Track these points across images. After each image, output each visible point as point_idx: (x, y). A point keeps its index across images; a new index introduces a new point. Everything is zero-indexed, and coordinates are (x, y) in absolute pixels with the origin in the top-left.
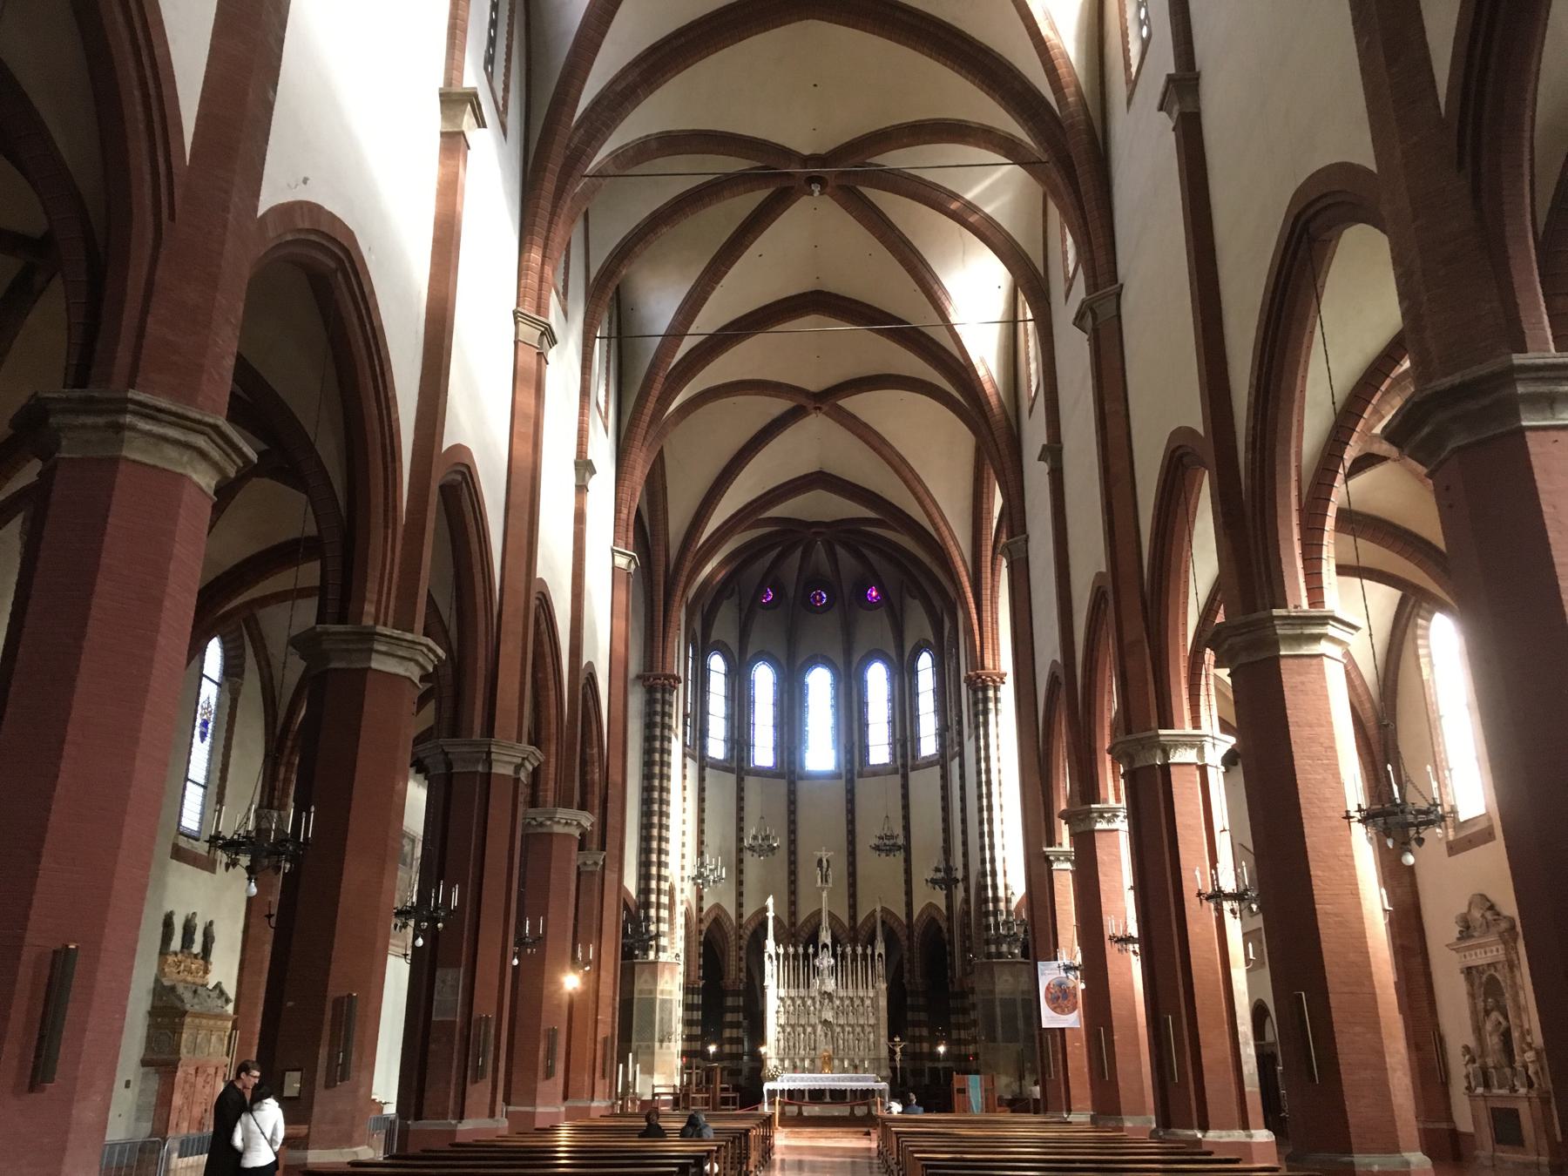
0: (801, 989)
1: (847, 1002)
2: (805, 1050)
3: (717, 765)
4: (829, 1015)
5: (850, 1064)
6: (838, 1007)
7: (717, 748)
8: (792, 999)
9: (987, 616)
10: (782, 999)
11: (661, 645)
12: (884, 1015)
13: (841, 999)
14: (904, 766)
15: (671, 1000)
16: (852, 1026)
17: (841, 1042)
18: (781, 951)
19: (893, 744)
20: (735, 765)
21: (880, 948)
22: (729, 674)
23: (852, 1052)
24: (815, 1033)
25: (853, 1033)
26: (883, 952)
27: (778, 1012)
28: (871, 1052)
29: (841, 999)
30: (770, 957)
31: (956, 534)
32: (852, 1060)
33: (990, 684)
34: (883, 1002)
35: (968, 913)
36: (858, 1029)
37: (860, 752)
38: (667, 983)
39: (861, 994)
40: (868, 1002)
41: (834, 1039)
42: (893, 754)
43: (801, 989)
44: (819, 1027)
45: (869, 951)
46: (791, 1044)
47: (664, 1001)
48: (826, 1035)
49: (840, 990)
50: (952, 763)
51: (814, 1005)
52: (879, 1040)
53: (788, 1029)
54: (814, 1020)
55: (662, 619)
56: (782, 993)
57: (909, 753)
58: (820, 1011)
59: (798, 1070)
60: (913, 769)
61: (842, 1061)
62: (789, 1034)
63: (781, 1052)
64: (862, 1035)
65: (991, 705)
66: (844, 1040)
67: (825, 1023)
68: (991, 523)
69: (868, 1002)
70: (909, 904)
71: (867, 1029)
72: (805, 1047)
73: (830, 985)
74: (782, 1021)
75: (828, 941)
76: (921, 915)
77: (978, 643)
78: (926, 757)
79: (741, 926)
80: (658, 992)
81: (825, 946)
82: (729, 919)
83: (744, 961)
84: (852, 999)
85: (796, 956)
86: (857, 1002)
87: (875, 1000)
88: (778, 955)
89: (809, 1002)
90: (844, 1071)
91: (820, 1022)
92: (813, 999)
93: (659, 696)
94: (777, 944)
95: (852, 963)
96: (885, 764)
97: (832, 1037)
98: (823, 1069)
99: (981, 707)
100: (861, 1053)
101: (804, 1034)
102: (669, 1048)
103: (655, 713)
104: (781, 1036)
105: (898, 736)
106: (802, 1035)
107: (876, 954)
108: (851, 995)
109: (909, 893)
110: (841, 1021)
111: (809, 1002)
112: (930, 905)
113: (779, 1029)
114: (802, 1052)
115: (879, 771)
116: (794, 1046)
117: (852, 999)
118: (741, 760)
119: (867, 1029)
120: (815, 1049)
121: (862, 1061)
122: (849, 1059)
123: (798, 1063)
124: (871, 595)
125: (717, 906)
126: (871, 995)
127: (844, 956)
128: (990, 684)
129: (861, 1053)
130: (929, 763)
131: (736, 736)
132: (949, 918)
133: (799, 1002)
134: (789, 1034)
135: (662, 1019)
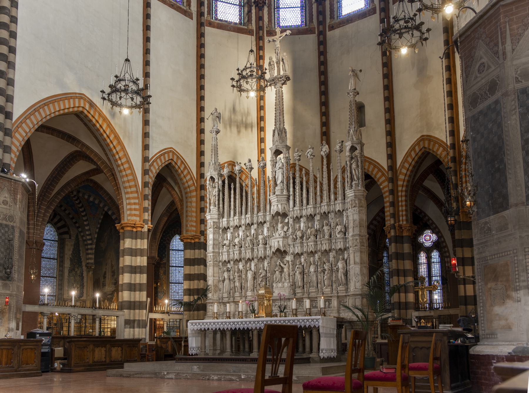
46: (237, 284)
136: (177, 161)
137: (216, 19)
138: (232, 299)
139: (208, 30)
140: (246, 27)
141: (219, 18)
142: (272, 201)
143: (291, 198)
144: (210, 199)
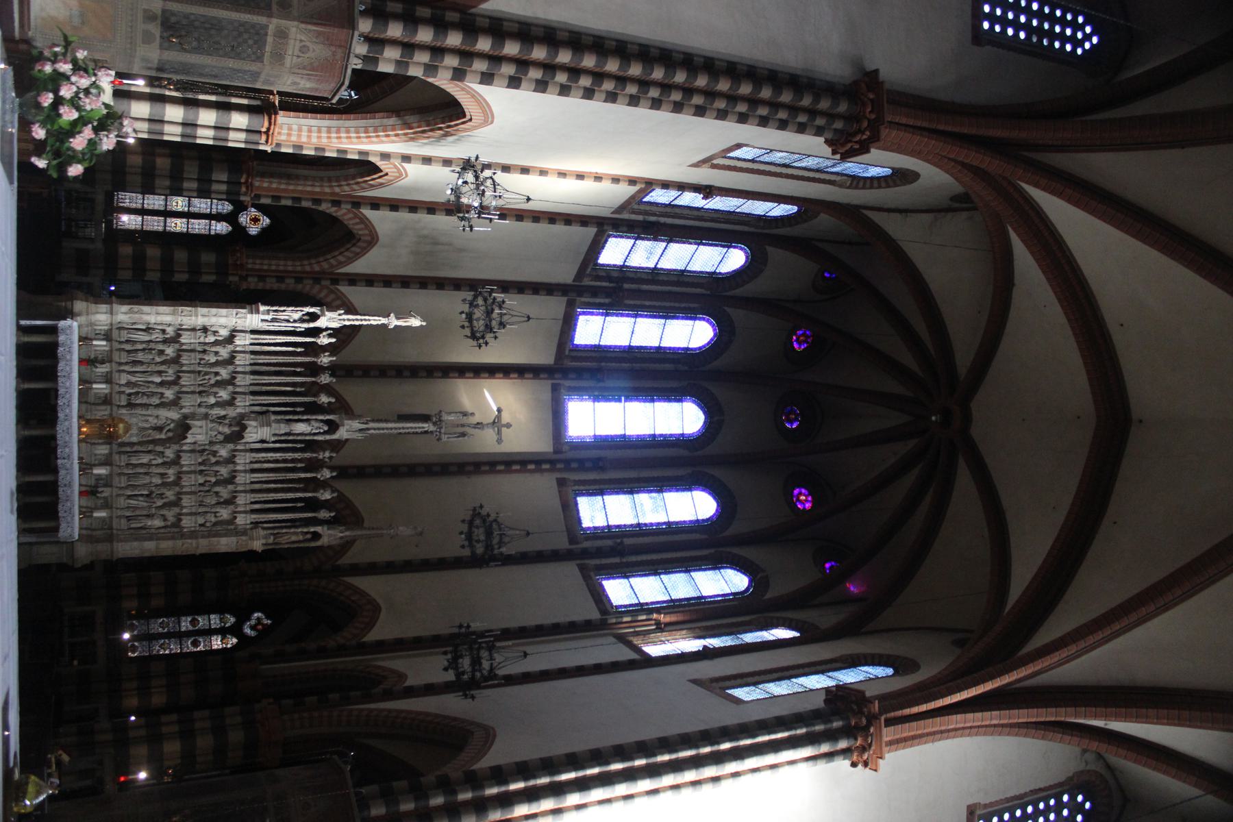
0: (249, 379)
1: (224, 471)
2: (129, 384)
3: (597, 246)
4: (199, 434)
5: (99, 478)
6: (214, 453)
7: (615, 252)
8: (230, 360)
9: (957, 720)
10: (230, 339)
11: (919, 124)
12: (203, 546)
13: (230, 460)
14: (585, 554)
15: (259, 59)
16: (177, 482)
17: (145, 459)
18: (324, 340)
19: (609, 533)
20: (587, 282)
21: (329, 536)
22: (713, 280)
23: (123, 482)
24: (162, 405)
25: (164, 484)
26: (324, 541)
27: (205, 330)
28: (123, 521)
29: (230, 460)
30: (313, 317)
31: (1083, 658)
32: (107, 482)
33: (859, 742)
34: (226, 544)
35: (389, 695)
36: (170, 495)
37: (594, 482)
38: (304, 49)
39: (241, 500)
40: (224, 513)
41: (149, 444)
42: (599, 534)
43: (249, 379)
44: (174, 415)
45: (324, 514)
46: (140, 356)
47: (259, 34)
48: (159, 429)
49: (249, 457)
50: (612, 640)
51: (217, 404)
52: (150, 539)
53: (170, 351)
54: (189, 404)
55: (957, 130)
56: (242, 341)
57: (604, 561)
58: (206, 416)
59: (86, 370)
60: (583, 569)
61: (107, 462)
62: (161, 352)
63: (125, 336)
64: (160, 503)
65: (825, 748)
66: (149, 465)
67: (183, 428)
68: (1096, 717)
69: (224, 513)
70: (373, 569)
71: (170, 514)
72: (134, 385)
73: (256, 433)
74: (186, 339)
75: (342, 433)
76: (357, 590)
77: (915, 710)
78: (604, 590)
79: (336, 280)
80: (283, 22)
81: (333, 427)
82: (350, 261)
83: (276, 286)
84: (231, 480)
85: (314, 370)
86: (224, 492)
87: (228, 527)
88: (316, 332)
89: (224, 394)
90: (85, 467)
91: (185, 417)
92: (230, 403)
93: (843, 107)
94: (335, 332)
95: (299, 480)
96: (579, 521)
97: (154, 442)
98: (89, 422)
99: (819, 728)
100: (122, 502)
101: (162, 384)
102: (148, 38)
103: (817, 98)
104: (156, 336)
105: (627, 541)
106: (158, 380)
107: (319, 529)
108: (240, 479)
109: (390, 568)
110: (186, 460)
111: (224, 394)
112: (377, 609)
113: (170, 331)
114: (124, 379)
115: (570, 513)
116: (135, 363)
117: (231, 480)
118: (595, 292)
119: (170, 514)
120: (130, 405)
121: (106, 505)
122: (111, 475)
123: (102, 369)
124: (800, 494)
125: (373, 239)
126: (241, 520)
127: (314, 465)
128: (859, 742)
129: (122, 502)
130: (600, 598)
131: (626, 286)
132: (364, 648)
133: (224, 373)
134: (161, 352)
135: (215, 26)
136: (359, 247)
137: (609, 236)
138: (116, 345)
139: (592, 231)
140: (588, 272)
141: (610, 239)
142: (264, 416)
143: (265, 445)
144: (284, 311)
